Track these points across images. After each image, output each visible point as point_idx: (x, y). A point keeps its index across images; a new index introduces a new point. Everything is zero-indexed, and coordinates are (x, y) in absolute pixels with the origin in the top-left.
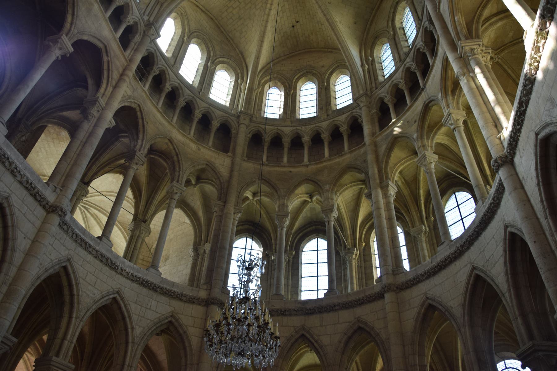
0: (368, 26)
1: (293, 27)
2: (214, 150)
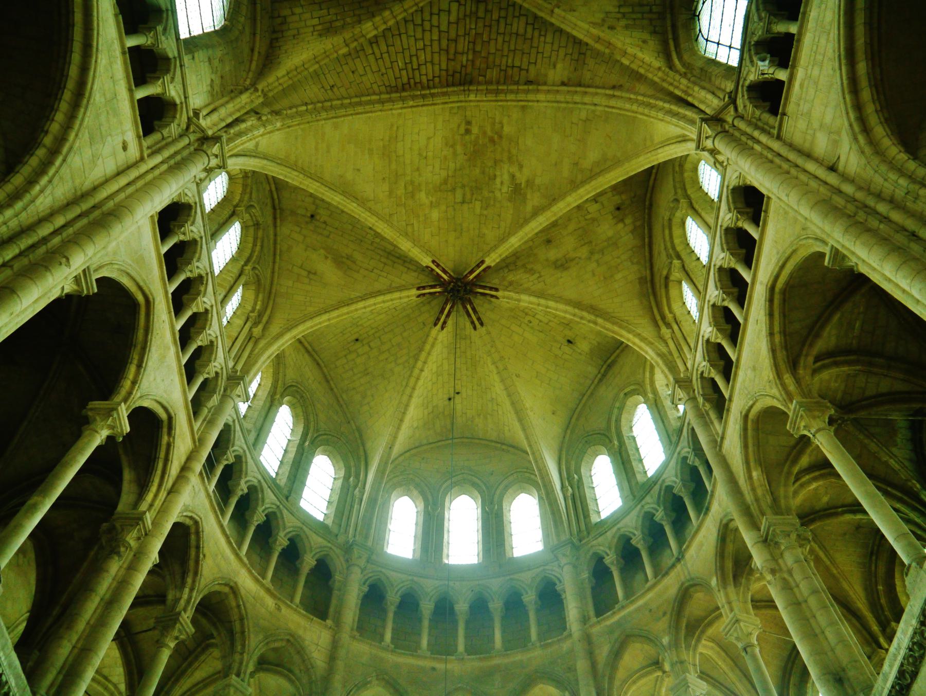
0: (573, 420)
2: (305, 613)
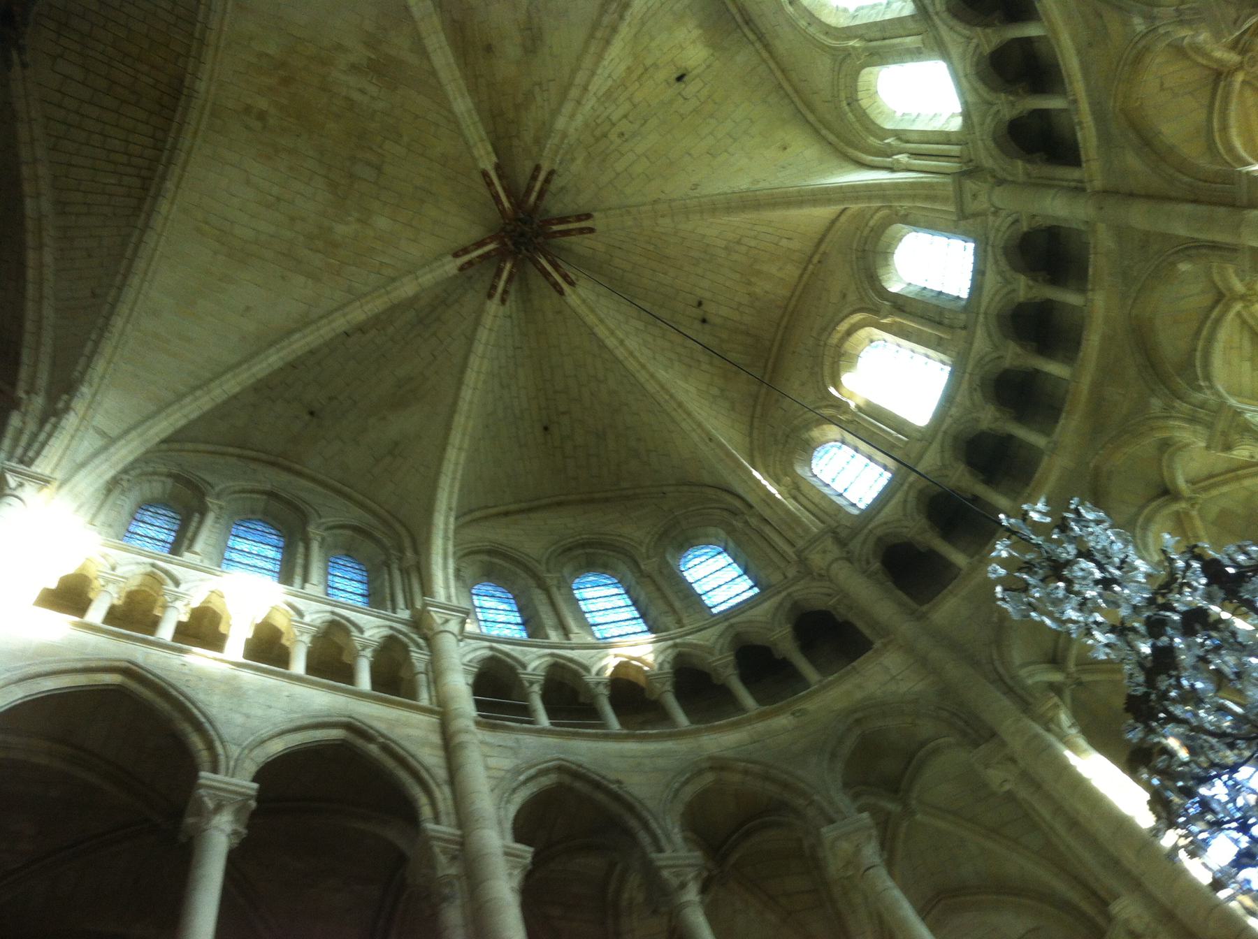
0: (811, 117)
1: (704, 321)
2: (836, 675)
